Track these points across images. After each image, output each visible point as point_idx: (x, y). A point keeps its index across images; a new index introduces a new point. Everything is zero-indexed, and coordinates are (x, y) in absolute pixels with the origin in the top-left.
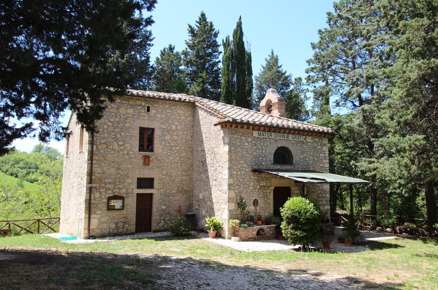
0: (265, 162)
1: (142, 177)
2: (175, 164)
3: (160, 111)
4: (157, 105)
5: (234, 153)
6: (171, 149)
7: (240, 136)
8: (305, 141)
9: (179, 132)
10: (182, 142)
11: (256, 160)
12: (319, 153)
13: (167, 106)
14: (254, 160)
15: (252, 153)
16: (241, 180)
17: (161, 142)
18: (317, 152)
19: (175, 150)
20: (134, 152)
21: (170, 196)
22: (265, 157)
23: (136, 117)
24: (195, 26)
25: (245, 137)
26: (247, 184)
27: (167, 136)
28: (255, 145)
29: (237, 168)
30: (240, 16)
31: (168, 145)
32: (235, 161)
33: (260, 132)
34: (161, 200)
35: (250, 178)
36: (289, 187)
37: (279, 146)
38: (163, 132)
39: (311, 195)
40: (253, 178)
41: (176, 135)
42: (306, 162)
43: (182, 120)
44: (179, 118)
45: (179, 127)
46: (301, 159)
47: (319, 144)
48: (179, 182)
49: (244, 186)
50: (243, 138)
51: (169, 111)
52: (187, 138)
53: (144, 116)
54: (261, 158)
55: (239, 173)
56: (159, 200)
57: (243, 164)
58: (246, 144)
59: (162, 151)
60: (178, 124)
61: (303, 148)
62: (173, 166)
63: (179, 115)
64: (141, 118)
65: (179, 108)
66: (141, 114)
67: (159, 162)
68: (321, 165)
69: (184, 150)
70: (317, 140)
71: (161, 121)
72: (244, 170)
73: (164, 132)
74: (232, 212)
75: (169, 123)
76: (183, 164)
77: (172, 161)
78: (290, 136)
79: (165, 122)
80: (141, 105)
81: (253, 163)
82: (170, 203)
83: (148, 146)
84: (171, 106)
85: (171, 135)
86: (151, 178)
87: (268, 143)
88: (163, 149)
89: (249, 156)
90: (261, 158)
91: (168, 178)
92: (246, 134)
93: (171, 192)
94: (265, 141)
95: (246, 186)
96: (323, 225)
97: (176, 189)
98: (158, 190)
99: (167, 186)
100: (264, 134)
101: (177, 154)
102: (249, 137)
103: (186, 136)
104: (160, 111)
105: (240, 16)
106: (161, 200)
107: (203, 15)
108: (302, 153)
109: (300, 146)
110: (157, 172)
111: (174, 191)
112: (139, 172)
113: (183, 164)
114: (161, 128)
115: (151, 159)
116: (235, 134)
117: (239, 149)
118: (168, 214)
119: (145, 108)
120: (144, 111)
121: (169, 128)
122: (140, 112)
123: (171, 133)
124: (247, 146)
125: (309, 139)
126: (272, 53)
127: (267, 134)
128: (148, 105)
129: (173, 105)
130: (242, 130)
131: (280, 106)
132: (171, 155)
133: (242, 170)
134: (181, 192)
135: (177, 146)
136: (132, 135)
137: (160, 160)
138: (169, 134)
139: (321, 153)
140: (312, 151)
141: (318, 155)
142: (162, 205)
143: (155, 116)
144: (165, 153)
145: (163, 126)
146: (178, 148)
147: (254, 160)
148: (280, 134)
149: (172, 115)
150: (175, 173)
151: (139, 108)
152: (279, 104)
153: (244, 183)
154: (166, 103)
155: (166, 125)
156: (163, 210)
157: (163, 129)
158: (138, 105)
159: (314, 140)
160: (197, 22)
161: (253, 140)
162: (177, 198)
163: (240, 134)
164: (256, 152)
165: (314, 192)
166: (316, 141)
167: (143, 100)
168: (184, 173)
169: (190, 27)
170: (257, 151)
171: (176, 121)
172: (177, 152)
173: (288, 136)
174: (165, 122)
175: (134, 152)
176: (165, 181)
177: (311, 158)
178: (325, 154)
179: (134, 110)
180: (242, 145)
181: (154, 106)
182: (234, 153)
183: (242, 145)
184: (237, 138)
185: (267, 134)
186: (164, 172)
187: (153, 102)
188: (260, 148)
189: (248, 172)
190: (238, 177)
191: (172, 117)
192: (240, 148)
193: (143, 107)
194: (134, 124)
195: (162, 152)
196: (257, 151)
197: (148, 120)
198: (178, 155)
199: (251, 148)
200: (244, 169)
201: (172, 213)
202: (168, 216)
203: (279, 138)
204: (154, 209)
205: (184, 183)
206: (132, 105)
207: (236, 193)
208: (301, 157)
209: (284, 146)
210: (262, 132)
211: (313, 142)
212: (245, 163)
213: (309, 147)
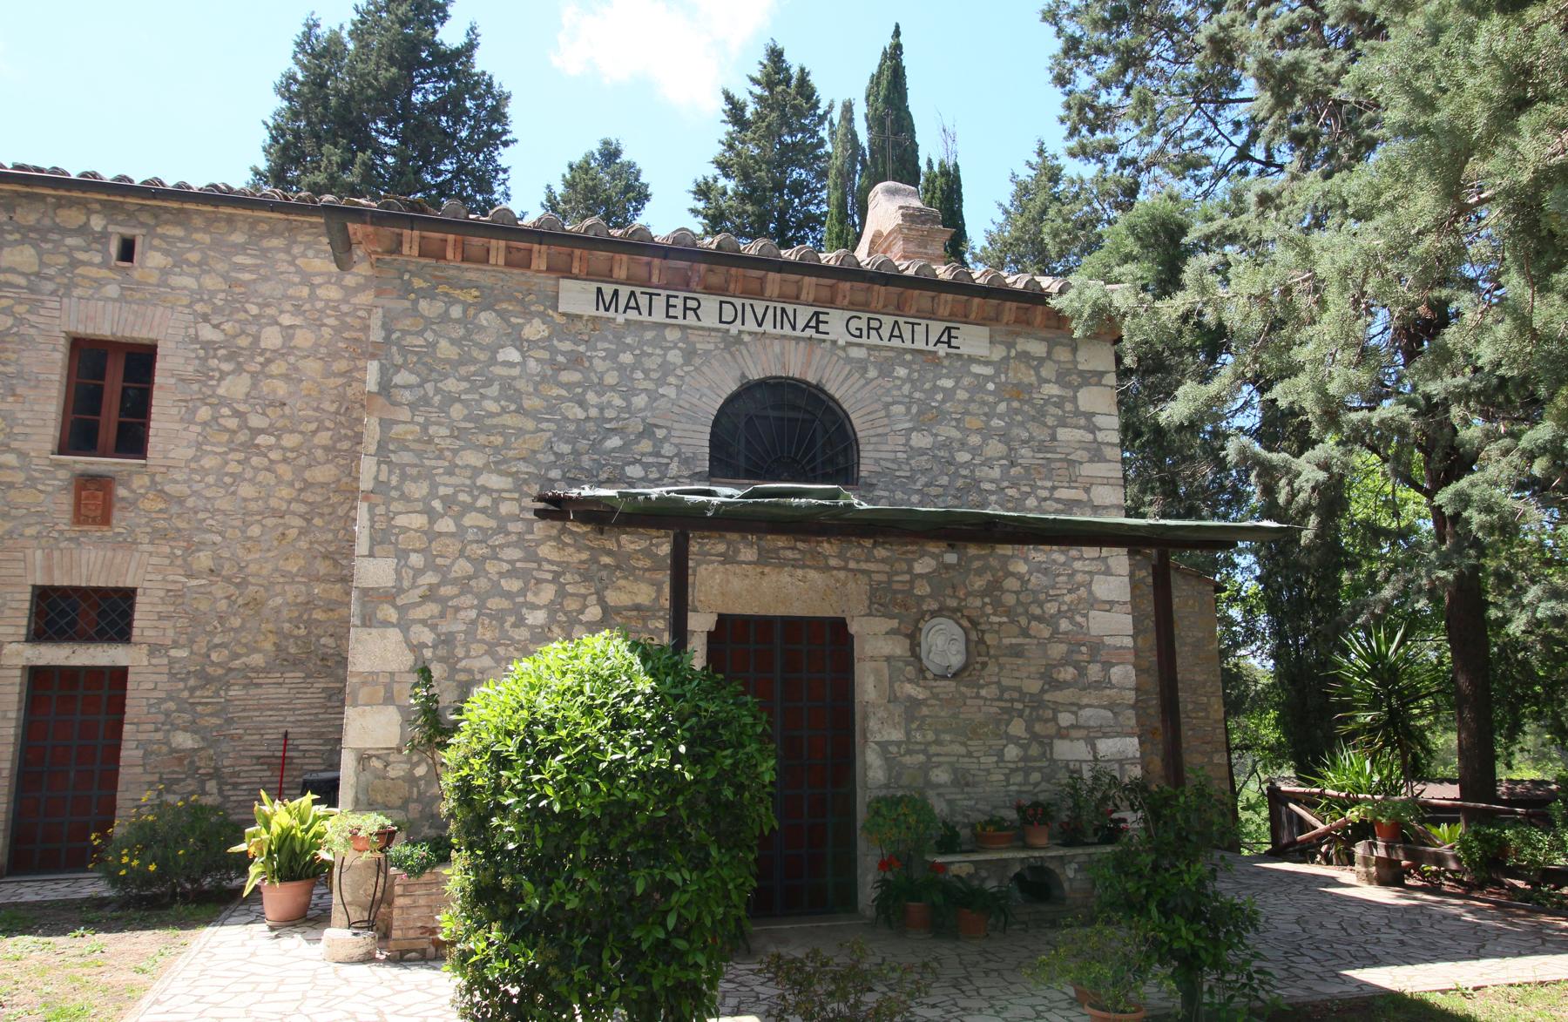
0: (646, 466)
1: (60, 580)
2: (270, 522)
3: (194, 257)
4: (178, 232)
5: (413, 406)
6: (250, 447)
7: (466, 306)
8: (942, 350)
9: (301, 364)
10: (317, 409)
11: (576, 453)
12: (1050, 421)
13: (238, 238)
14: (565, 448)
15: (551, 409)
16: (462, 567)
17: (194, 411)
18: (1039, 417)
19: (270, 448)
20: (22, 455)
21: (228, 686)
22: (648, 431)
23: (50, 286)
24: (744, 92)
25: (502, 315)
26: (508, 595)
27: (225, 383)
28: (575, 361)
29: (433, 493)
30: (897, 27)
31: (232, 423)
32: (420, 454)
33: (608, 290)
34: (172, 705)
35: (531, 556)
36: (844, 619)
37: (755, 374)
39: (992, 668)
40: (555, 556)
41: (286, 377)
42: (956, 475)
43: (320, 305)
44: (305, 291)
45: (304, 339)
46: (922, 452)
47: (1048, 371)
49: (481, 607)
50: (485, 318)
51: (248, 261)
52: (349, 391)
53: (95, 280)
54: (615, 442)
55: (446, 525)
56: (162, 701)
57: (477, 472)
58: (512, 355)
59: (191, 452)
60: (298, 321)
61: (935, 389)
62: (255, 531)
63: (306, 278)
64: (77, 292)
65: (308, 246)
66: (79, 271)
67: (175, 509)
68: (1063, 494)
69: (326, 449)
70: (1037, 348)
71: (199, 307)
72: (483, 510)
73: (213, 363)
74: (376, 764)
75: (242, 316)
76: (317, 521)
77: (253, 506)
78: (836, 324)
79: (217, 310)
80: (83, 230)
81: (553, 465)
82: (229, 721)
83: (122, 429)
84: (263, 236)
85: (254, 375)
86: (117, 590)
87: (675, 357)
88: (199, 446)
89: (530, 425)
90: (615, 442)
91: (219, 590)
92: (511, 298)
93: (237, 663)
94: (651, 343)
95: (495, 603)
96: (1061, 860)
97: (268, 646)
98: (155, 649)
99: (212, 634)
100: (643, 301)
101: (282, 469)
102: (528, 315)
103: (340, 381)
104: (194, 257)
105: (897, 27)
106: (172, 705)
107: (776, 55)
108: (926, 418)
109: (909, 379)
110: (154, 560)
111: (257, 659)
112: (49, 557)
113: (317, 521)
114: (196, 339)
115: (121, 492)
116: (429, 294)
117: (451, 385)
118: (211, 776)
119: (106, 245)
120: (98, 259)
121: (243, 342)
122: (75, 263)
123: (254, 367)
124: (511, 365)
125: (973, 340)
126: (1041, 152)
127: (660, 303)
128: (127, 231)
129: (272, 233)
130: (472, 273)
131: (912, 247)
132: (249, 474)
133: (467, 508)
134: (296, 663)
135: (284, 430)
136: (19, 375)
137: (181, 501)
138: (239, 369)
139: (1063, 424)
140: (1002, 407)
141: (1041, 434)
142: (176, 728)
143: (163, 283)
144: (208, 462)
145: (207, 333)
146: (290, 440)
147: (565, 448)
148: (760, 307)
149: (266, 279)
150: (269, 566)
151: (70, 241)
152: (906, 240)
153: (483, 583)
154: (230, 220)
155: (226, 326)
156: (180, 756)
157: (208, 345)
158: (65, 231)
159: (1010, 346)
160: (754, 81)
161: (558, 333)
162: (271, 692)
164: (582, 404)
165: (1017, 651)
166: (1025, 356)
167: (97, 207)
168: (322, 567)
169: (729, 98)
170: (591, 397)
171: (287, 306)
172: (285, 460)
173: (817, 321)
174: (217, 310)
175: (22, 455)
176: (204, 606)
177: (995, 448)
178: (1093, 429)
179: (40, 254)
180: (475, 361)
181: (163, 237)
182: (413, 406)
183: (475, 361)
184: (445, 318)
185: (660, 303)
186: (204, 560)
187: (156, 217)
188: (611, 378)
189: (517, 518)
190: (436, 547)
191: (265, 288)
192: (466, 379)
193: (96, 240)
194: (33, 318)
195: (196, 459)
196: (591, 397)
197: (122, 299)
198: (288, 476)
199: (544, 378)
200: (484, 501)
201: (236, 774)
202: (211, 786)
203: (751, 325)
204: (129, 752)
205: (318, 615)
206: (32, 229)
207: (416, 648)
208: (920, 440)
209: (794, 371)
210: (624, 291)
211: (1006, 359)
212: (498, 467)
213: (981, 388)
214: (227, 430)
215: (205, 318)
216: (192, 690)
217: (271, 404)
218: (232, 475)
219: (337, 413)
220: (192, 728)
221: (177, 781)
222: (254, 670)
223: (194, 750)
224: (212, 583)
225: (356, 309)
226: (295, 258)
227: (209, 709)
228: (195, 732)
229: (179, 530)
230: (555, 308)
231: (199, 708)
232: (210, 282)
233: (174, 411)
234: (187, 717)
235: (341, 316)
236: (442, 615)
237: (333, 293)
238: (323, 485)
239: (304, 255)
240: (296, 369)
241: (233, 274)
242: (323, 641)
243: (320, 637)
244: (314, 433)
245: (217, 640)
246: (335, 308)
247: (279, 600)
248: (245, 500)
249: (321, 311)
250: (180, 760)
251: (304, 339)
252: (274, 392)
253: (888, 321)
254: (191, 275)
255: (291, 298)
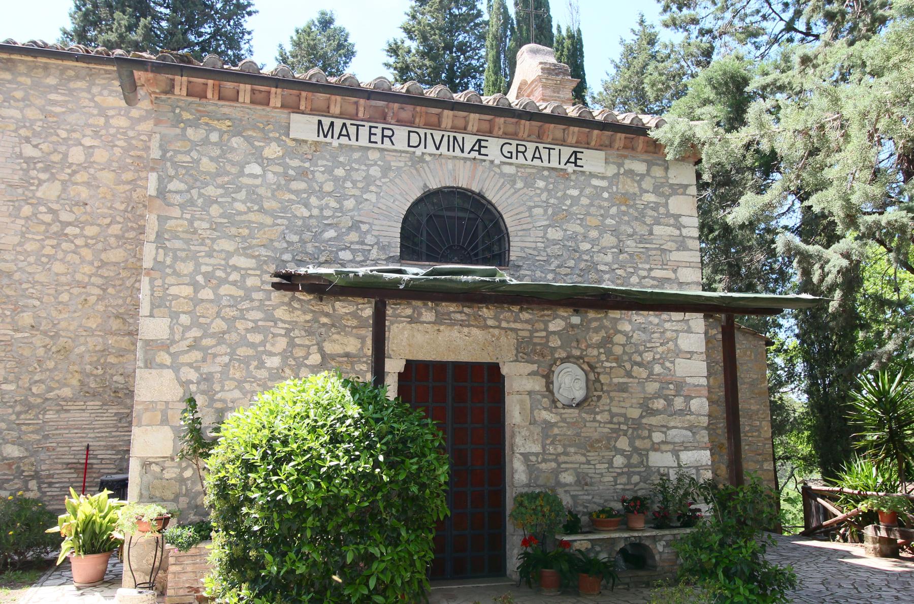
0: (354, 252)
2: (76, 291)
3: (19, 94)
5: (182, 206)
6: (61, 235)
7: (222, 133)
8: (571, 168)
9: (99, 174)
10: (111, 208)
11: (303, 242)
12: (648, 220)
13: (52, 81)
14: (295, 238)
15: (284, 209)
16: (219, 325)
17: (19, 209)
19: (76, 236)
21: (45, 411)
22: (355, 226)
25: (248, 139)
26: (253, 345)
28: (303, 174)
29: (197, 271)
31: (48, 218)
32: (187, 242)
33: (326, 122)
37: (434, 185)
38: (26, 171)
39: (605, 400)
40: (287, 317)
41: (88, 184)
42: (580, 259)
43: (112, 131)
44: (102, 121)
45: (101, 156)
46: (555, 242)
47: (647, 184)
48: (87, 358)
49: (232, 354)
50: (236, 142)
51: (59, 98)
52: (135, 195)
54: (331, 233)
55: (207, 294)
57: (229, 255)
58: (256, 169)
59: (17, 239)
60: (96, 143)
61: (565, 196)
62: (65, 297)
63: (103, 112)
65: (104, 87)
69: (117, 237)
70: (640, 167)
71: (23, 132)
72: (234, 283)
73: (33, 173)
74: (155, 468)
75: (54, 138)
76: (111, 290)
77: (63, 279)
78: (493, 147)
79: (36, 134)
82: (46, 437)
84: (70, 79)
85: (64, 183)
87: (375, 171)
88: (23, 235)
89: (269, 221)
90: (331, 233)
91: (38, 341)
92: (255, 128)
93: (51, 395)
95: (242, 351)
96: (654, 539)
97: (75, 382)
99: (33, 373)
100: (352, 130)
101: (85, 252)
102: (267, 139)
103: (128, 187)
104: (19, 94)
108: (559, 218)
109: (546, 189)
111: (67, 392)
113: (111, 290)
114: (20, 156)
116: (195, 124)
118: (33, 477)
121: (56, 158)
124: (256, 176)
126: (642, 22)
127: (364, 132)
129: (77, 77)
130: (226, 108)
131: (549, 92)
132: (60, 255)
133: (223, 281)
134: (94, 395)
135: (86, 223)
138: (53, 178)
140: (614, 210)
141: (642, 230)
144: (29, 247)
145: (29, 151)
146: (91, 231)
147: (295, 238)
148: (438, 135)
149: (72, 111)
150: (75, 324)
152: (545, 87)
153: (234, 337)
154: (46, 67)
155: (44, 146)
157: (29, 160)
159: (620, 165)
161: (289, 153)
162: (76, 416)
163: (224, 125)
164: (307, 205)
165: (623, 388)
166: (630, 173)
168: (115, 324)
170: (313, 201)
171: (88, 132)
172: (87, 245)
173: (479, 146)
174: (36, 134)
176: (27, 353)
177: (609, 240)
178: (679, 227)
180: (228, 173)
182: (182, 206)
183: (228, 173)
184: (206, 141)
185: (364, 132)
186: (27, 318)
189: (259, 289)
190: (199, 310)
191: (72, 118)
192: (221, 186)
195: (20, 244)
196: (313, 201)
198: (89, 257)
199: (279, 186)
200: (235, 276)
201: (51, 476)
202: (33, 484)
203: (431, 148)
205: (112, 359)
207: (185, 384)
208: (554, 234)
209: (463, 183)
210: (338, 123)
211: (617, 175)
212: (245, 251)
213: (599, 196)
214: (43, 223)
215: (27, 140)
216: (18, 414)
217: (77, 204)
218: (47, 256)
219: (126, 211)
220: (18, 442)
221: (8, 481)
222: (64, 400)
223: (20, 458)
224: (33, 336)
225: (140, 135)
226: (94, 96)
227: (31, 428)
228: (20, 445)
229: (8, 296)
230: (288, 135)
231: (24, 428)
232: (31, 113)
233: (4, 208)
234: (15, 434)
235: (128, 140)
236: (204, 360)
237: (123, 122)
238: (116, 264)
239: (101, 94)
240: (95, 178)
241: (49, 108)
242: (115, 378)
243: (112, 376)
244: (109, 225)
245: (37, 378)
246: (124, 134)
247: (83, 348)
248: (57, 274)
249: (114, 136)
250: (10, 466)
251: (101, 156)
252: (79, 194)
253: (531, 147)
254: (17, 108)
255: (90, 126)
